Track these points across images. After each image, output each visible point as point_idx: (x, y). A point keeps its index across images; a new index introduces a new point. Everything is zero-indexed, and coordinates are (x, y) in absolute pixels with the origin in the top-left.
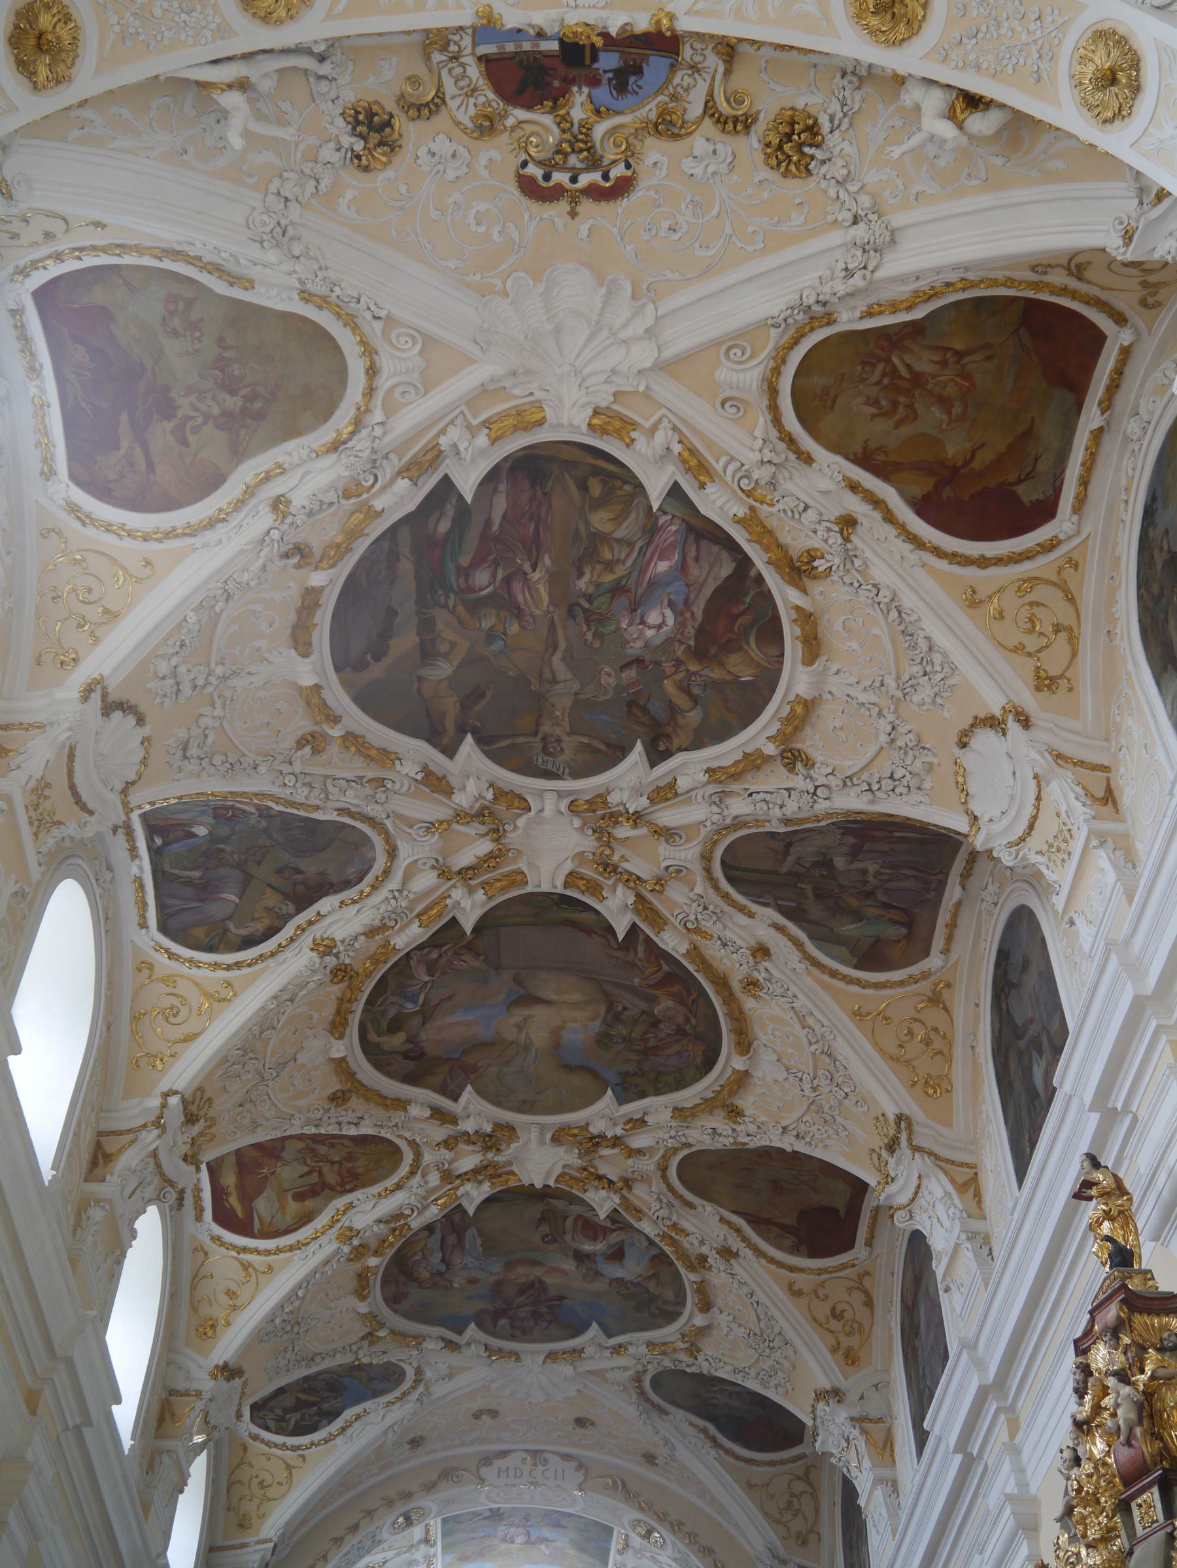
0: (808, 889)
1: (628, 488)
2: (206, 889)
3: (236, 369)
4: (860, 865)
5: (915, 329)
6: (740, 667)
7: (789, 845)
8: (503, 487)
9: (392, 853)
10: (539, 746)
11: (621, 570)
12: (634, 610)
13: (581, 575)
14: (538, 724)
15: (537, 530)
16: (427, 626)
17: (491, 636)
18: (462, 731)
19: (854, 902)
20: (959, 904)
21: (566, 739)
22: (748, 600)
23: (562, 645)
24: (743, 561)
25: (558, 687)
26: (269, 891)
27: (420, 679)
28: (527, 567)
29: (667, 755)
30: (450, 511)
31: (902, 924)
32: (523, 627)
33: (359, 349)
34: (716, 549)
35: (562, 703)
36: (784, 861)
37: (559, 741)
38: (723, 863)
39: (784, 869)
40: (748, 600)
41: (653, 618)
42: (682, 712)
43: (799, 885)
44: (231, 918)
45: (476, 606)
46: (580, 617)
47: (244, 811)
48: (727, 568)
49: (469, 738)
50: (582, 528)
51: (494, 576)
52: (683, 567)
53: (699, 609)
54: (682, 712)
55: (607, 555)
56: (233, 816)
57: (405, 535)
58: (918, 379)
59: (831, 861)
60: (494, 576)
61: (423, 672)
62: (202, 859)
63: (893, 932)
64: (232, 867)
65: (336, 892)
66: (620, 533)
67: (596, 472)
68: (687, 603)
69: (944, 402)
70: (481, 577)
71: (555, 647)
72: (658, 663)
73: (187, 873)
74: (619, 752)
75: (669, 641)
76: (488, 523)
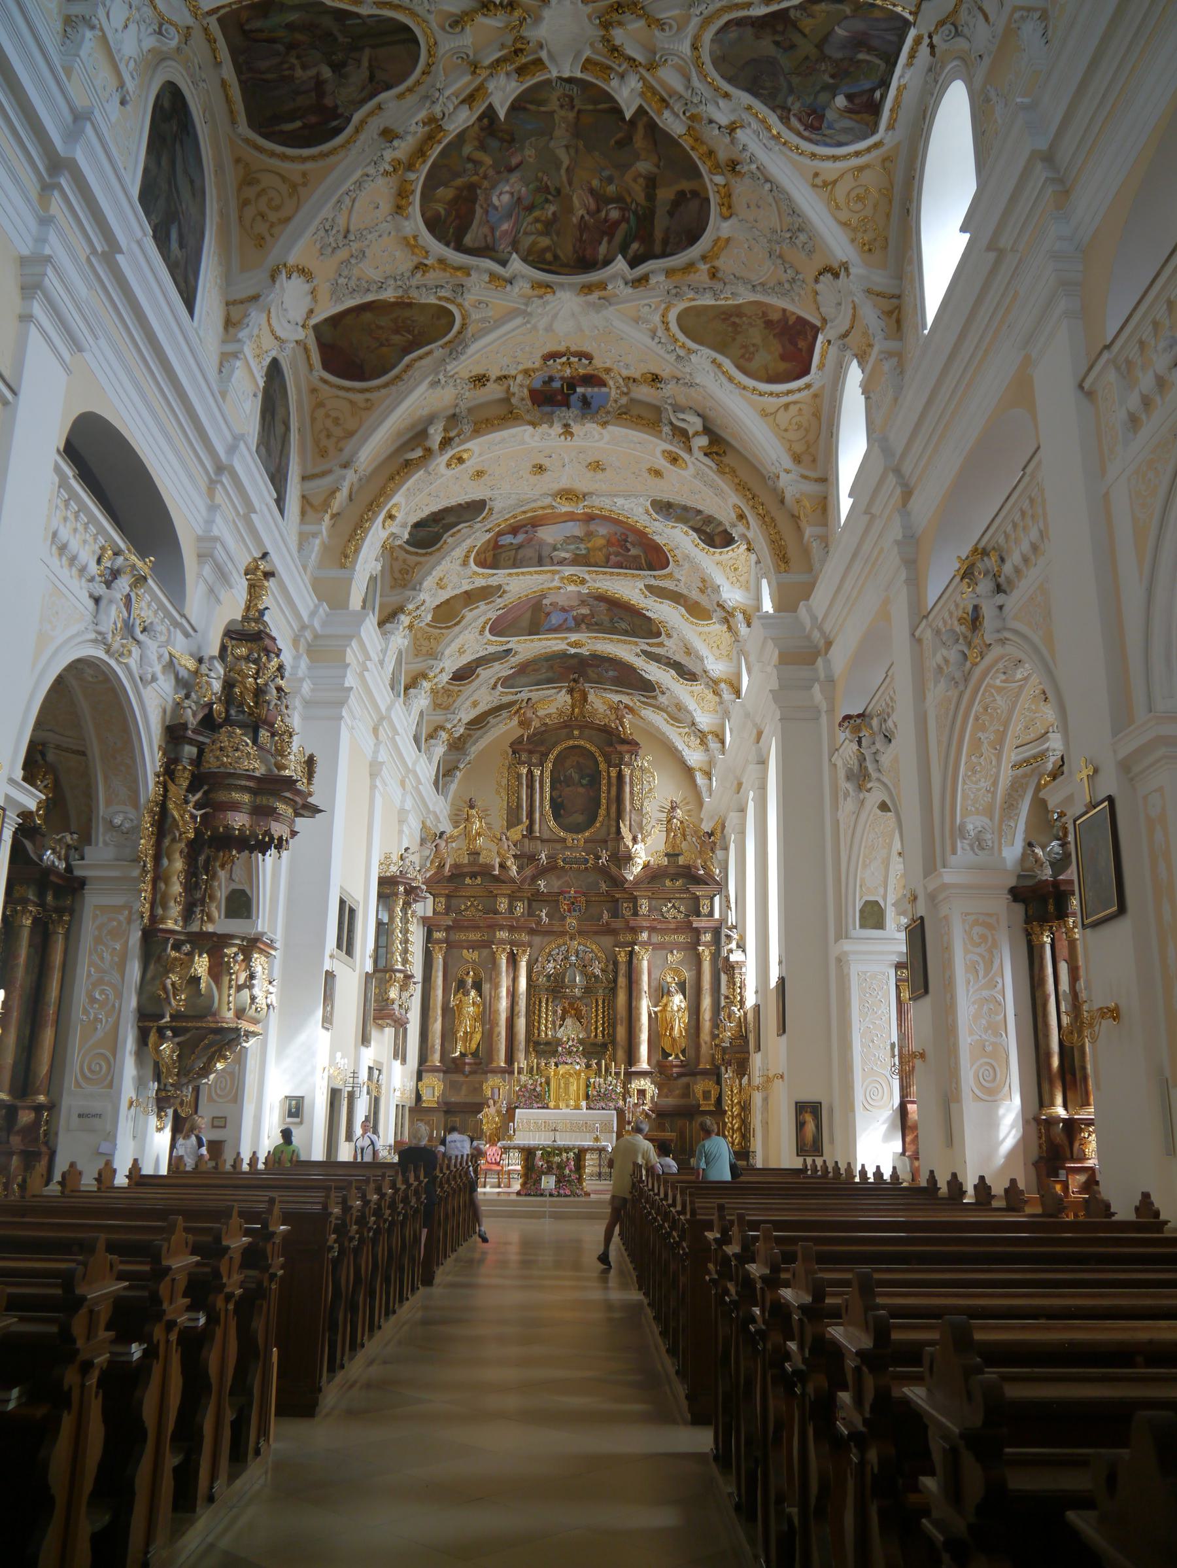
0: (341, 39)
1: (531, 258)
2: (859, 42)
3: (730, 329)
4: (312, 72)
5: (407, 351)
6: (445, 193)
7: (372, 78)
8: (601, 257)
9: (695, 47)
10: (577, 102)
11: (530, 219)
12: (519, 199)
13: (554, 214)
14: (578, 118)
15: (581, 236)
16: (651, 197)
17: (610, 180)
18: (633, 122)
19: (299, 37)
20: (233, 122)
21: (556, 108)
22: (451, 230)
23: (563, 172)
24: (460, 248)
25: (564, 143)
26: (807, 31)
27: (658, 167)
28: (587, 217)
29: (480, 119)
30: (631, 252)
31: (251, 31)
32: (589, 183)
33: (670, 325)
34: (476, 245)
35: (561, 134)
36: (370, 60)
37: (562, 106)
38: (416, 42)
39: (367, 52)
40: (451, 230)
41: (506, 198)
42: (476, 149)
43: (349, 40)
44: (846, 18)
45: (619, 199)
46: (552, 190)
47: (800, 120)
48: (468, 240)
49: (628, 116)
50: (555, 238)
51: (607, 214)
52: (493, 230)
53: (479, 211)
54: (476, 149)
55: (539, 226)
56: (809, 115)
57: (658, 248)
58: (397, 331)
59: (334, 72)
60: (607, 214)
61: (655, 170)
62: (852, 69)
63: (258, 24)
64: (830, 58)
65: (749, 17)
66: (532, 238)
67: (550, 263)
68: (487, 212)
69: (379, 327)
70: (615, 214)
71: (567, 169)
72: (499, 173)
73: (868, 58)
74: (516, 107)
75: (493, 187)
76: (609, 242)
